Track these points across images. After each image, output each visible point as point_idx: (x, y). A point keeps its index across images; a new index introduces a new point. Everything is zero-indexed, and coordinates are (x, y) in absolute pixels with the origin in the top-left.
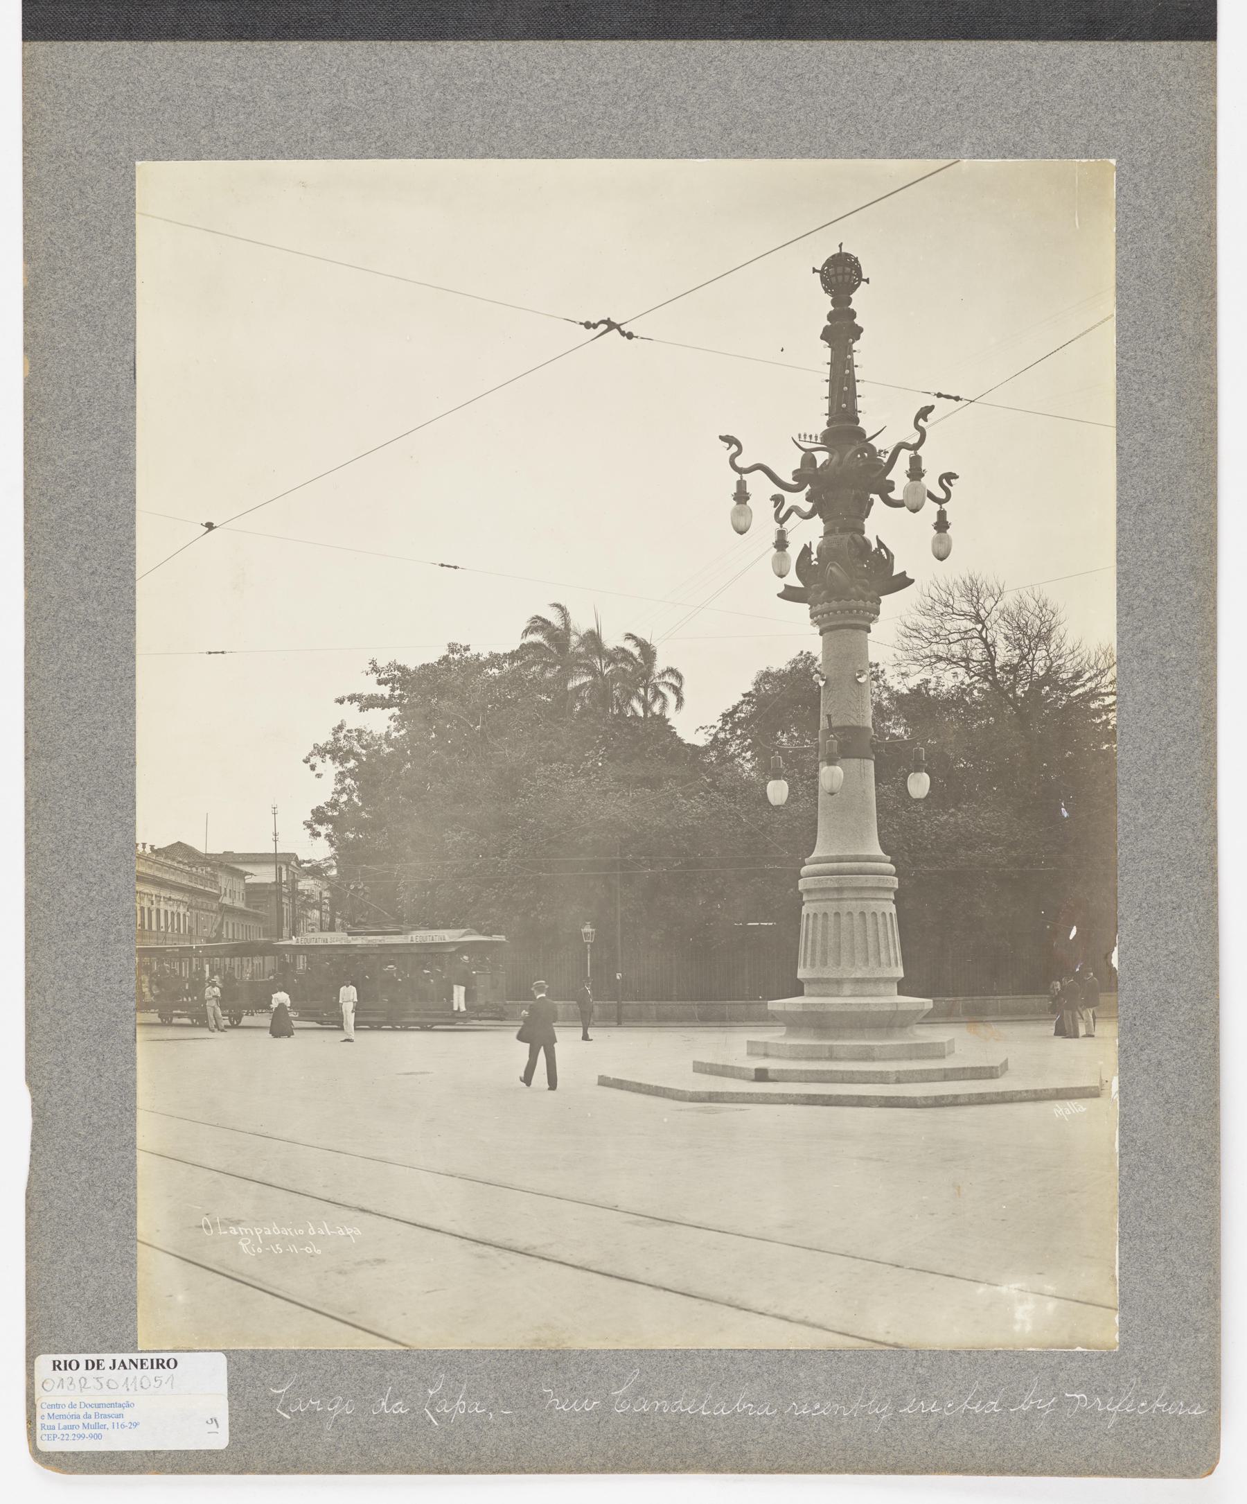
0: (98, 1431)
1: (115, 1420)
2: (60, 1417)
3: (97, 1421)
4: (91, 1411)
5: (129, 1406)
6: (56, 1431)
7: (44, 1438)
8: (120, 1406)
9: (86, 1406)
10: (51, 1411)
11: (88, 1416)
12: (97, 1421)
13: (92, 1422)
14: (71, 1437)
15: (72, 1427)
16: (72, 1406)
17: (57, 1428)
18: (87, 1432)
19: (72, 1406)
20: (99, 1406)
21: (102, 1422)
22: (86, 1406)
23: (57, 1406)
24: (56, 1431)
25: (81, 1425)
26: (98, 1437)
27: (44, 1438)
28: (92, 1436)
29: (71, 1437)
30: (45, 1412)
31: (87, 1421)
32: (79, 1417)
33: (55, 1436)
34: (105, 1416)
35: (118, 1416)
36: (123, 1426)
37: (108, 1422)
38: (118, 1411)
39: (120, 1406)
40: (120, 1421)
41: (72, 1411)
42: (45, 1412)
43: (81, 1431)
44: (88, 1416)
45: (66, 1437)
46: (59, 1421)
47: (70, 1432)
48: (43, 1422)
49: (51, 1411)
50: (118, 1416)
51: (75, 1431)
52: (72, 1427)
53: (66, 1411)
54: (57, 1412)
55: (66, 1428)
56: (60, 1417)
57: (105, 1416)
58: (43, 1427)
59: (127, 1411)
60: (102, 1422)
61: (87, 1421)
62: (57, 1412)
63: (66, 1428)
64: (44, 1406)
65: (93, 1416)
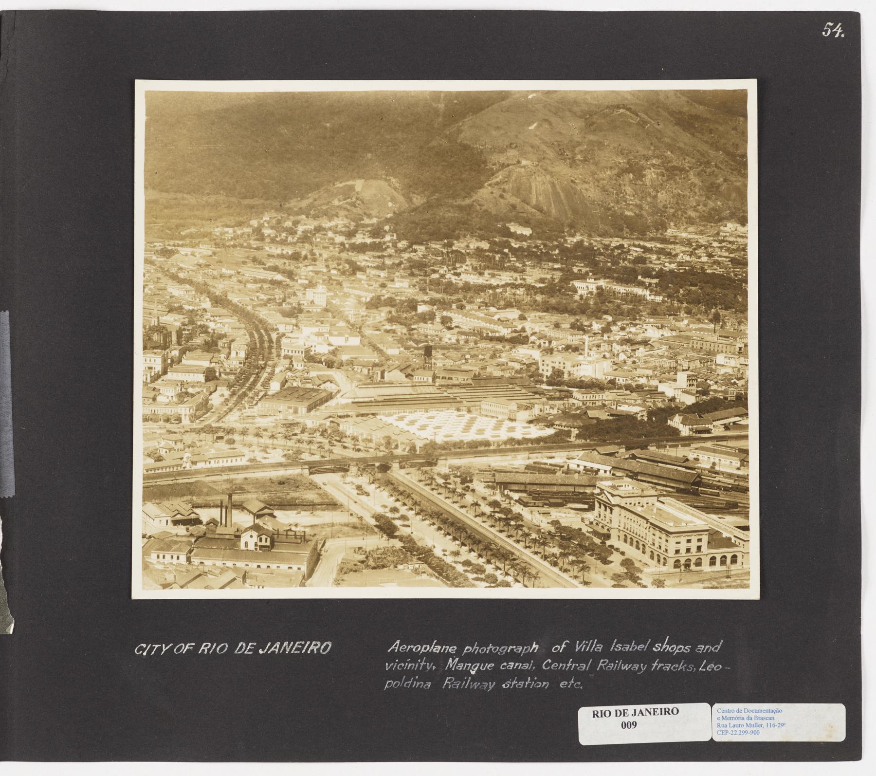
0: (756, 729)
1: (769, 722)
2: (731, 718)
3: (756, 721)
4: (752, 715)
5: (778, 711)
6: (728, 729)
7: (719, 733)
8: (773, 711)
9: (748, 711)
10: (725, 715)
11: (749, 718)
12: (756, 721)
13: (753, 722)
14: (738, 733)
15: (739, 726)
16: (739, 711)
17: (728, 726)
18: (749, 729)
19: (739, 711)
20: (757, 711)
21: (759, 722)
22: (748, 711)
23: (728, 711)
24: (728, 729)
25: (745, 725)
26: (757, 733)
27: (719, 733)
28: (753, 732)
29: (738, 733)
30: (720, 715)
31: (749, 722)
32: (744, 719)
33: (727, 732)
34: (762, 719)
35: (770, 719)
36: (774, 725)
37: (764, 723)
38: (771, 715)
39: (773, 711)
40: (772, 722)
41: (739, 715)
42: (720, 715)
43: (745, 728)
44: (749, 718)
45: (734, 733)
46: (730, 721)
47: (735, 729)
48: (718, 722)
49: (725, 715)
50: (770, 719)
51: (742, 729)
52: (739, 726)
53: (735, 715)
54: (729, 715)
55: (734, 726)
56: (731, 718)
57: (762, 719)
58: (718, 725)
59: (776, 715)
60: (759, 722)
61: (749, 722)
62: (729, 715)
63: (734, 726)
64: (720, 711)
65: (753, 718)
